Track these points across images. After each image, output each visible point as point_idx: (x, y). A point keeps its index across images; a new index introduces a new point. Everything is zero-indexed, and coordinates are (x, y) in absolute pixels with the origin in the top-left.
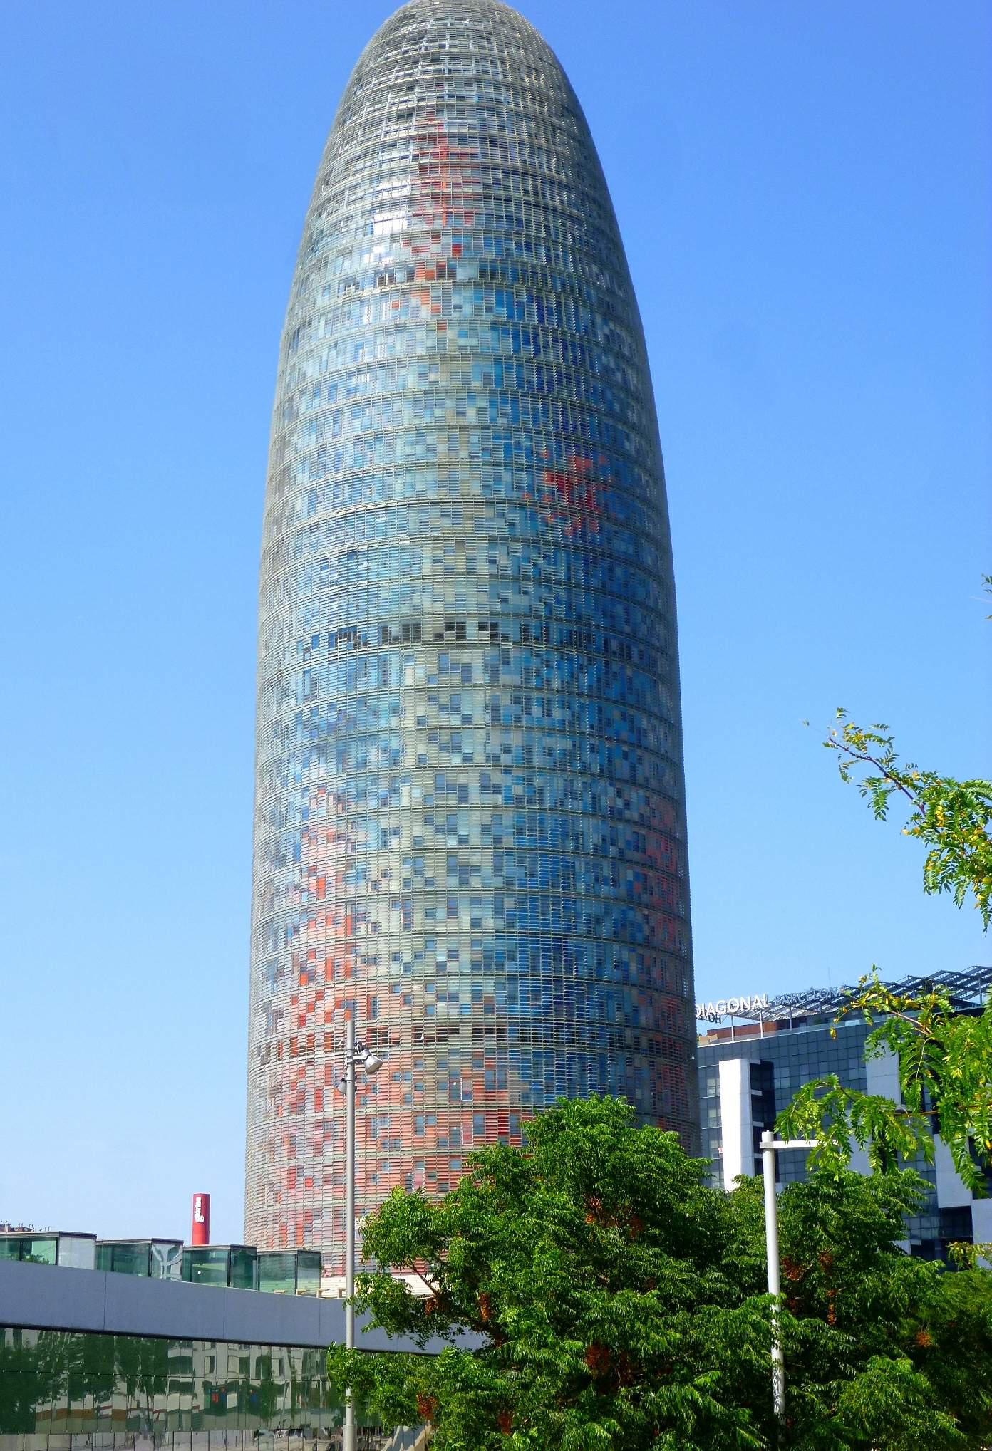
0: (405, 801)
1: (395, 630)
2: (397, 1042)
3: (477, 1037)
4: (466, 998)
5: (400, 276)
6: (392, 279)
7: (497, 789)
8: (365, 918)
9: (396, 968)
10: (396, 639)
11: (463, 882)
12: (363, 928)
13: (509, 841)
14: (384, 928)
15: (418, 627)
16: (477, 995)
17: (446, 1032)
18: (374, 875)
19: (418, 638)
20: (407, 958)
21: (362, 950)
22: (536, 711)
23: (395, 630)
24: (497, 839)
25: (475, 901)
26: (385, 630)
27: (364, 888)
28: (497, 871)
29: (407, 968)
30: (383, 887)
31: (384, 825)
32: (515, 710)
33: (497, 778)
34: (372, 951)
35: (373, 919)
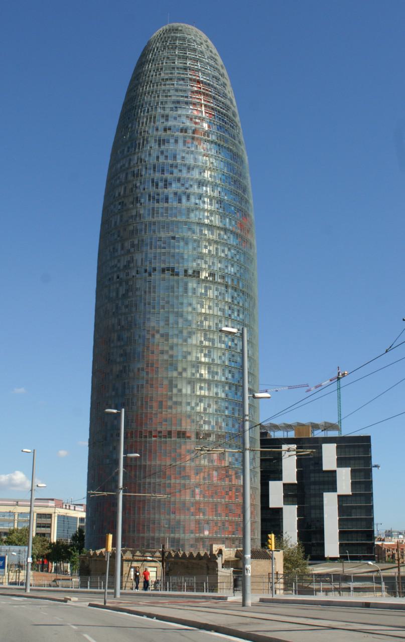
0: (194, 342)
1: (190, 272)
2: (189, 437)
3: (219, 437)
4: (213, 423)
5: (190, 132)
6: (186, 132)
7: (224, 342)
8: (176, 386)
9: (189, 408)
10: (190, 275)
11: (213, 377)
12: (175, 391)
13: (227, 363)
14: (184, 391)
15: (199, 273)
16: (217, 423)
17: (208, 435)
18: (180, 369)
19: (199, 277)
20: (193, 405)
21: (174, 399)
22: (236, 314)
23: (190, 272)
24: (224, 362)
25: (217, 386)
26: (186, 271)
27: (175, 374)
28: (224, 375)
29: (193, 408)
30: (184, 375)
31: (185, 349)
32: (230, 312)
33: (224, 338)
34: (179, 400)
35: (179, 387)
